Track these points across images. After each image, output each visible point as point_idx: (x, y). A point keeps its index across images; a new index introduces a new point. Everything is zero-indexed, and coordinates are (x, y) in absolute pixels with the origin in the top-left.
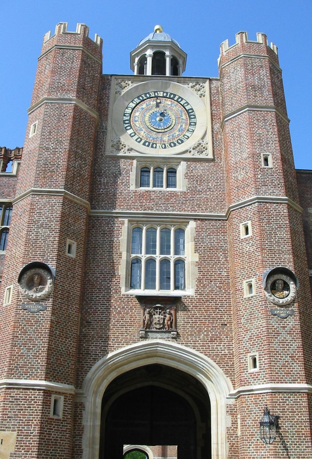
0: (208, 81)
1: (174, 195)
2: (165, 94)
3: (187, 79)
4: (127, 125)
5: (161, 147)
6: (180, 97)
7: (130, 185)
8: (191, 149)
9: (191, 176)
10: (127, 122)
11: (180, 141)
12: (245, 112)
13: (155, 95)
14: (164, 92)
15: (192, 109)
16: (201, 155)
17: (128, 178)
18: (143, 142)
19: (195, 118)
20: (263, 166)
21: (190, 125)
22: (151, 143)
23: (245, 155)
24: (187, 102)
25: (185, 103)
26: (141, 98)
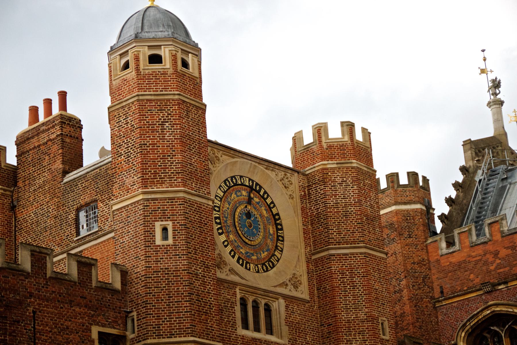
3: (277, 167)
4: (219, 226)
6: (265, 192)
8: (288, 282)
9: (290, 321)
10: (218, 221)
14: (250, 180)
15: (278, 214)
23: (362, 316)
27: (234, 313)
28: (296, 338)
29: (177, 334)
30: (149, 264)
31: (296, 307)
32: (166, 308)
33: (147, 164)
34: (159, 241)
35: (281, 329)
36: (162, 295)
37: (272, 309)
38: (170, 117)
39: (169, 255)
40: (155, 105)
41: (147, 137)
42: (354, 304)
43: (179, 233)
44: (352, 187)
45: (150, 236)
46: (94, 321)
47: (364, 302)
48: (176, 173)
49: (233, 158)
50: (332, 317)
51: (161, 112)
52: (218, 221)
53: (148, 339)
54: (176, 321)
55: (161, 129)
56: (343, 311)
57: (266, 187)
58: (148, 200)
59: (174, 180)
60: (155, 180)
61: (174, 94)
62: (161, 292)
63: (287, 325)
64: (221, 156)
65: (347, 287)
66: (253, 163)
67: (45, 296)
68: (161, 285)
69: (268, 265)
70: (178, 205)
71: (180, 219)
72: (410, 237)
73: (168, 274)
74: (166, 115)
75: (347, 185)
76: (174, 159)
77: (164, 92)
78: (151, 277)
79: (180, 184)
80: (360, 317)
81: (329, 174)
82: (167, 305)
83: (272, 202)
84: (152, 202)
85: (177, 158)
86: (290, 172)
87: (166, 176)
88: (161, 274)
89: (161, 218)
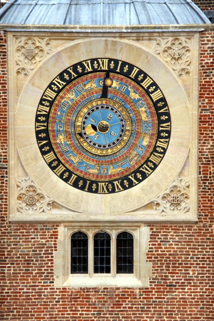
0: (197, 36)
1: (127, 293)
2: (112, 65)
5: (105, 189)
6: (141, 72)
7: (55, 277)
9: (158, 254)
11: (139, 176)
13: (93, 67)
16: (176, 212)
17: (50, 264)
18: (74, 177)
19: (169, 120)
21: (159, 137)
22: (88, 182)
24: (154, 84)
25: (152, 85)
26: (66, 77)
27: (52, 260)
49: (73, 40)
57: (140, 64)
63: (150, 261)
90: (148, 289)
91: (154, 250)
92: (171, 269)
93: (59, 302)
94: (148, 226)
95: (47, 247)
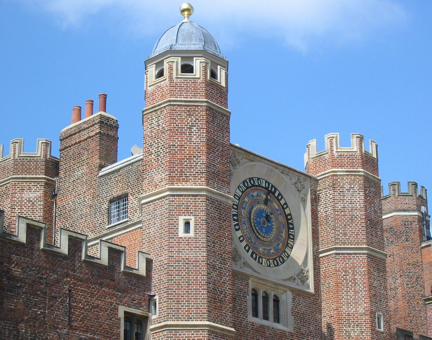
3: (291, 172)
4: (236, 223)
6: (280, 194)
7: (248, 314)
8: (296, 276)
9: (296, 312)
10: (235, 218)
12: (363, 254)
14: (266, 182)
15: (290, 215)
17: (245, 304)
20: (377, 329)
23: (361, 310)
27: (246, 302)
28: (300, 327)
29: (193, 318)
30: (171, 254)
31: (302, 300)
32: (185, 294)
33: (175, 163)
34: (181, 233)
35: (287, 318)
36: (183, 282)
37: (280, 300)
38: (197, 122)
39: (190, 247)
40: (185, 111)
41: (176, 139)
42: (354, 299)
43: (200, 227)
44: (358, 194)
45: (174, 229)
46: (121, 301)
47: (363, 298)
48: (200, 173)
49: (252, 161)
50: (334, 310)
51: (189, 117)
52: (235, 218)
53: (168, 320)
54: (194, 306)
55: (189, 132)
56: (344, 305)
58: (173, 196)
59: (198, 179)
60: (181, 178)
61: (202, 102)
62: (182, 280)
63: (293, 315)
64: (242, 159)
65: (349, 283)
66: (270, 167)
67: (79, 276)
68: (182, 273)
69: (278, 261)
70: (200, 201)
71: (202, 214)
72: (407, 241)
73: (189, 264)
74: (194, 120)
75: (354, 192)
76: (199, 160)
77: (193, 99)
78: (173, 266)
79: (204, 183)
80: (359, 311)
81: (339, 180)
82: (186, 292)
83: (286, 204)
84: (177, 198)
85: (202, 159)
86: (303, 176)
87: (191, 175)
88: (182, 264)
89: (184, 213)
90: (292, 333)
91: (294, 308)
92: (302, 323)
93: (250, 331)
94: (291, 292)
95: (244, 292)
